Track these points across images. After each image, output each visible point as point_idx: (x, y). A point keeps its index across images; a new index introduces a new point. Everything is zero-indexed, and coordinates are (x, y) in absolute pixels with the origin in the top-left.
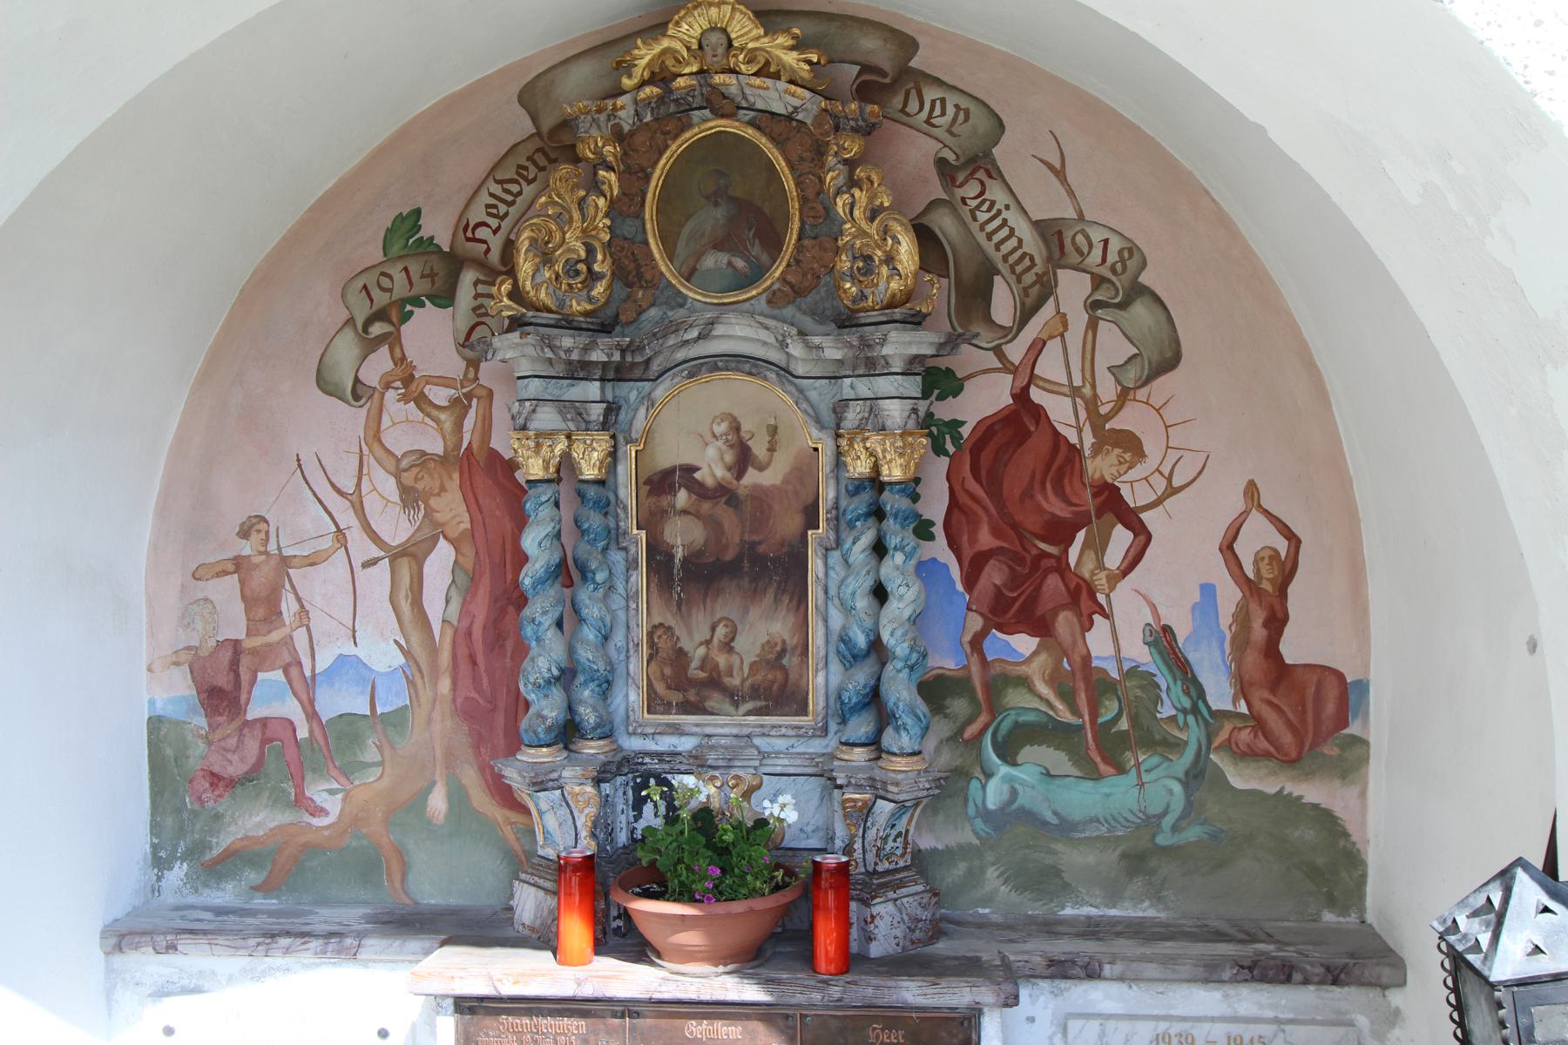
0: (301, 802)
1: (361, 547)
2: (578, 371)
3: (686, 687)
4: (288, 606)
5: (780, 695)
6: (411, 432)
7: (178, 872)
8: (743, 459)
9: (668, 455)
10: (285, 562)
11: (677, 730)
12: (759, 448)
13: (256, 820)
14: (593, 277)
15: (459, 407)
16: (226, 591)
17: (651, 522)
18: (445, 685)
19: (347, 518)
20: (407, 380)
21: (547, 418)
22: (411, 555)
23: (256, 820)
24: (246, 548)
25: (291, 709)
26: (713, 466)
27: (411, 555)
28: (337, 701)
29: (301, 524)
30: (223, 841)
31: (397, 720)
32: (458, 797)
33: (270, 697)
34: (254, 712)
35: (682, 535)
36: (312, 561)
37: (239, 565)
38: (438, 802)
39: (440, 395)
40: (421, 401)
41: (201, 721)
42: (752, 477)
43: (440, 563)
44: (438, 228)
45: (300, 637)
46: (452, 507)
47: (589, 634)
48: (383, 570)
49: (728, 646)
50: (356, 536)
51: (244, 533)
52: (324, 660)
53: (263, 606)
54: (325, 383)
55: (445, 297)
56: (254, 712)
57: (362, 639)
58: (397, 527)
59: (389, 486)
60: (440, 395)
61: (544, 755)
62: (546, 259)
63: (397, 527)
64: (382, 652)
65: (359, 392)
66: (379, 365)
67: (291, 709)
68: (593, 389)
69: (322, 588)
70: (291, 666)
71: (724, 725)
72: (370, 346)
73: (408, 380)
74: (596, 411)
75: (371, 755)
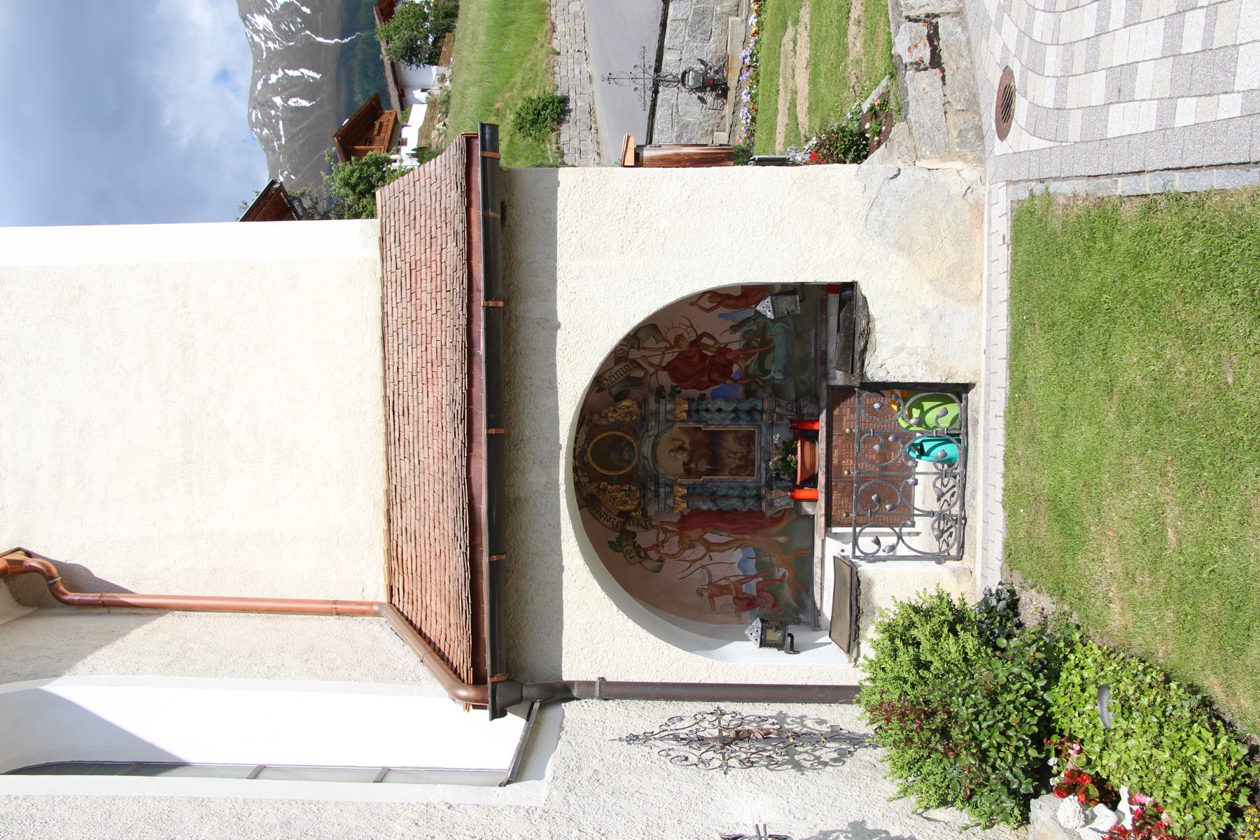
0: (781, 580)
1: (706, 561)
2: (657, 494)
3: (747, 465)
4: (723, 583)
5: (749, 438)
6: (673, 546)
7: (801, 616)
8: (681, 448)
9: (680, 470)
10: (710, 583)
11: (759, 468)
12: (678, 444)
13: (787, 593)
14: (630, 490)
15: (665, 531)
16: (719, 601)
17: (699, 475)
18: (747, 537)
19: (697, 565)
20: (657, 546)
21: (670, 502)
22: (709, 546)
23: (787, 593)
24: (706, 595)
25: (754, 583)
26: (683, 457)
27: (709, 546)
28: (752, 569)
29: (699, 578)
30: (793, 603)
31: (758, 552)
32: (780, 534)
33: (750, 589)
34: (755, 594)
35: (703, 466)
36: (710, 575)
37: (711, 597)
38: (782, 539)
39: (662, 537)
40: (663, 542)
41: (757, 609)
42: (686, 446)
43: (710, 537)
44: (614, 536)
45: (733, 579)
46: (695, 534)
47: (731, 492)
48: (713, 555)
49: (735, 453)
50: (704, 562)
51: (702, 595)
52: (739, 572)
53: (723, 590)
54: (658, 570)
55: (634, 535)
56: (755, 594)
57: (732, 561)
58: (700, 550)
59: (688, 552)
60: (662, 537)
61: (764, 504)
62: (625, 502)
63: (700, 550)
64: (737, 555)
65: (661, 560)
66: (652, 554)
67: (754, 583)
68: (662, 490)
69: (718, 573)
70: (741, 582)
71: (757, 455)
72: (647, 557)
73: (657, 546)
74: (668, 489)
75: (767, 559)
